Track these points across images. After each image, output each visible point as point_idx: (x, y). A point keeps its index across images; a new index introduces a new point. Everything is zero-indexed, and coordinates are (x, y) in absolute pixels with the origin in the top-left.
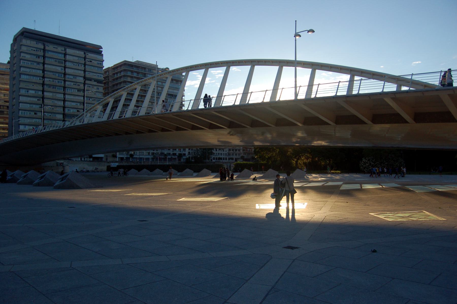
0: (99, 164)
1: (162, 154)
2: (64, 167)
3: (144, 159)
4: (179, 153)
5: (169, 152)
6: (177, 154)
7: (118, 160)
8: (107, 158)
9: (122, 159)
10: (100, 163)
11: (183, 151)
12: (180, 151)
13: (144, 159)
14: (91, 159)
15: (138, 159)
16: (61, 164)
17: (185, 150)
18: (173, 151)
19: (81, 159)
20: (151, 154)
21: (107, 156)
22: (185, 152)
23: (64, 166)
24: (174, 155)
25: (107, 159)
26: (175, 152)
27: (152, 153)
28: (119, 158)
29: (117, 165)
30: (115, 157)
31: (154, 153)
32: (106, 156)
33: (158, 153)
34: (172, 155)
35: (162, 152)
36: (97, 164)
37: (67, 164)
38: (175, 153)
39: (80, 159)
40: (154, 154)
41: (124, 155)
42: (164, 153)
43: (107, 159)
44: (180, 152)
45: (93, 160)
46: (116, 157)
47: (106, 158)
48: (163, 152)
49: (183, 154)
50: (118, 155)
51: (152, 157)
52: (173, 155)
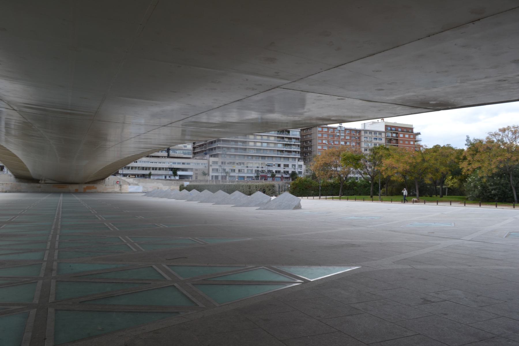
0: (177, 183)
1: (269, 171)
2: (121, 186)
3: (245, 178)
4: (293, 170)
5: (278, 169)
6: (290, 172)
7: (211, 179)
8: (197, 177)
9: (217, 177)
10: (179, 182)
11: (298, 169)
12: (295, 168)
13: (245, 178)
14: (177, 178)
15: (237, 178)
16: (118, 183)
17: (301, 167)
18: (284, 168)
19: (166, 177)
20: (254, 172)
21: (197, 174)
22: (302, 169)
23: (121, 185)
24: (285, 173)
25: (196, 178)
26: (287, 169)
27: (255, 170)
28: (212, 176)
29: (188, 184)
30: (207, 176)
31: (258, 171)
32: (196, 174)
33: (264, 170)
34: (282, 173)
35: (268, 169)
36: (175, 183)
37: (137, 183)
38: (287, 171)
39: (164, 178)
40: (258, 172)
41: (220, 174)
42: (272, 171)
43: (196, 178)
44: (295, 169)
45: (180, 178)
46: (209, 175)
47: (196, 176)
48: (271, 169)
49: (299, 172)
50: (211, 174)
51: (256, 175)
52: (284, 173)
